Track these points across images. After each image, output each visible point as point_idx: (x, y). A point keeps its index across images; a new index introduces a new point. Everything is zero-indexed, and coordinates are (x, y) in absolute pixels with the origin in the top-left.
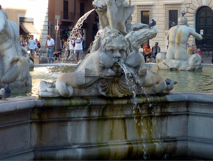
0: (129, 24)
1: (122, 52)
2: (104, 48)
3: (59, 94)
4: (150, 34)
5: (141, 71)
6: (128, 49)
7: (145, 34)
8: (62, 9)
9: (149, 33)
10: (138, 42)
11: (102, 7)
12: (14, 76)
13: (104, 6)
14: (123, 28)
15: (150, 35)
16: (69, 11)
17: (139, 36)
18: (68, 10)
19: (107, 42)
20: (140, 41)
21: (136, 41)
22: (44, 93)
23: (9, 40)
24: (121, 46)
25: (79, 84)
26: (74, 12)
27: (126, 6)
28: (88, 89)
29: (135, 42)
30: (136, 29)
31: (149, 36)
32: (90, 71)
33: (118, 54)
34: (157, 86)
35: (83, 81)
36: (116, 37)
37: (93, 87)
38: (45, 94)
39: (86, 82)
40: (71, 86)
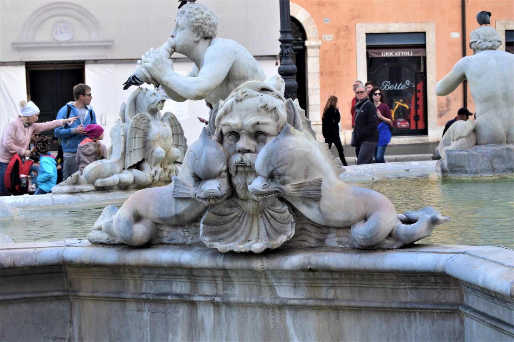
1: (262, 137)
24: (250, 120)
36: (241, 100)
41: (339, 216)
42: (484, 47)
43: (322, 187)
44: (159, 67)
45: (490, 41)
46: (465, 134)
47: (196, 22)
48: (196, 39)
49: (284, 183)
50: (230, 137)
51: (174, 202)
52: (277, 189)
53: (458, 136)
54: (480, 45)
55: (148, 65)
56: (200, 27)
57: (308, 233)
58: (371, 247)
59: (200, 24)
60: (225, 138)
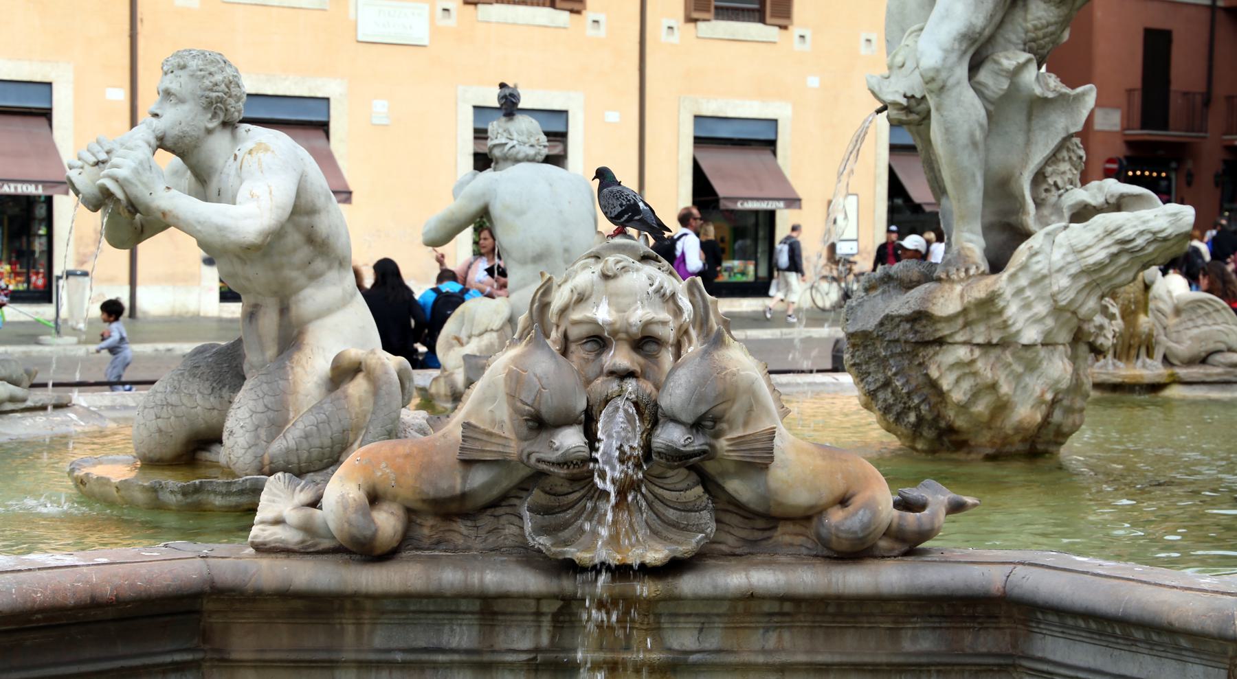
0: (1055, 184)
1: (651, 347)
2: (558, 326)
3: (334, 538)
4: (1149, 236)
5: (738, 442)
6: (686, 332)
7: (1119, 236)
8: (1133, 75)
9: (1141, 233)
10: (1084, 280)
11: (904, 102)
12: (327, 442)
13: (918, 96)
14: (1021, 208)
15: (1149, 243)
16: (1175, 86)
17: (1089, 247)
18: (1167, 82)
19: (575, 297)
20: (1095, 277)
21: (1074, 277)
22: (266, 533)
23: (332, 275)
24: (639, 315)
25: (432, 493)
26: (1200, 87)
27: (1038, 91)
28: (486, 521)
29: (1063, 281)
30: (1082, 214)
31: (1142, 249)
32: (485, 438)
33: (620, 357)
34: (836, 517)
35: (454, 483)
36: (615, 276)
37: (508, 510)
38: (275, 534)
39: (468, 487)
40: (394, 499)
41: (801, 497)
42: (521, 155)
43: (777, 441)
44: (145, 179)
45: (532, 146)
46: (497, 324)
47: (211, 90)
48: (211, 125)
49: (717, 435)
50: (588, 346)
51: (459, 467)
52: (706, 447)
53: (482, 328)
54: (514, 150)
55: (122, 173)
56: (221, 100)
57: (727, 528)
58: (857, 551)
59: (220, 94)
60: (573, 347)
